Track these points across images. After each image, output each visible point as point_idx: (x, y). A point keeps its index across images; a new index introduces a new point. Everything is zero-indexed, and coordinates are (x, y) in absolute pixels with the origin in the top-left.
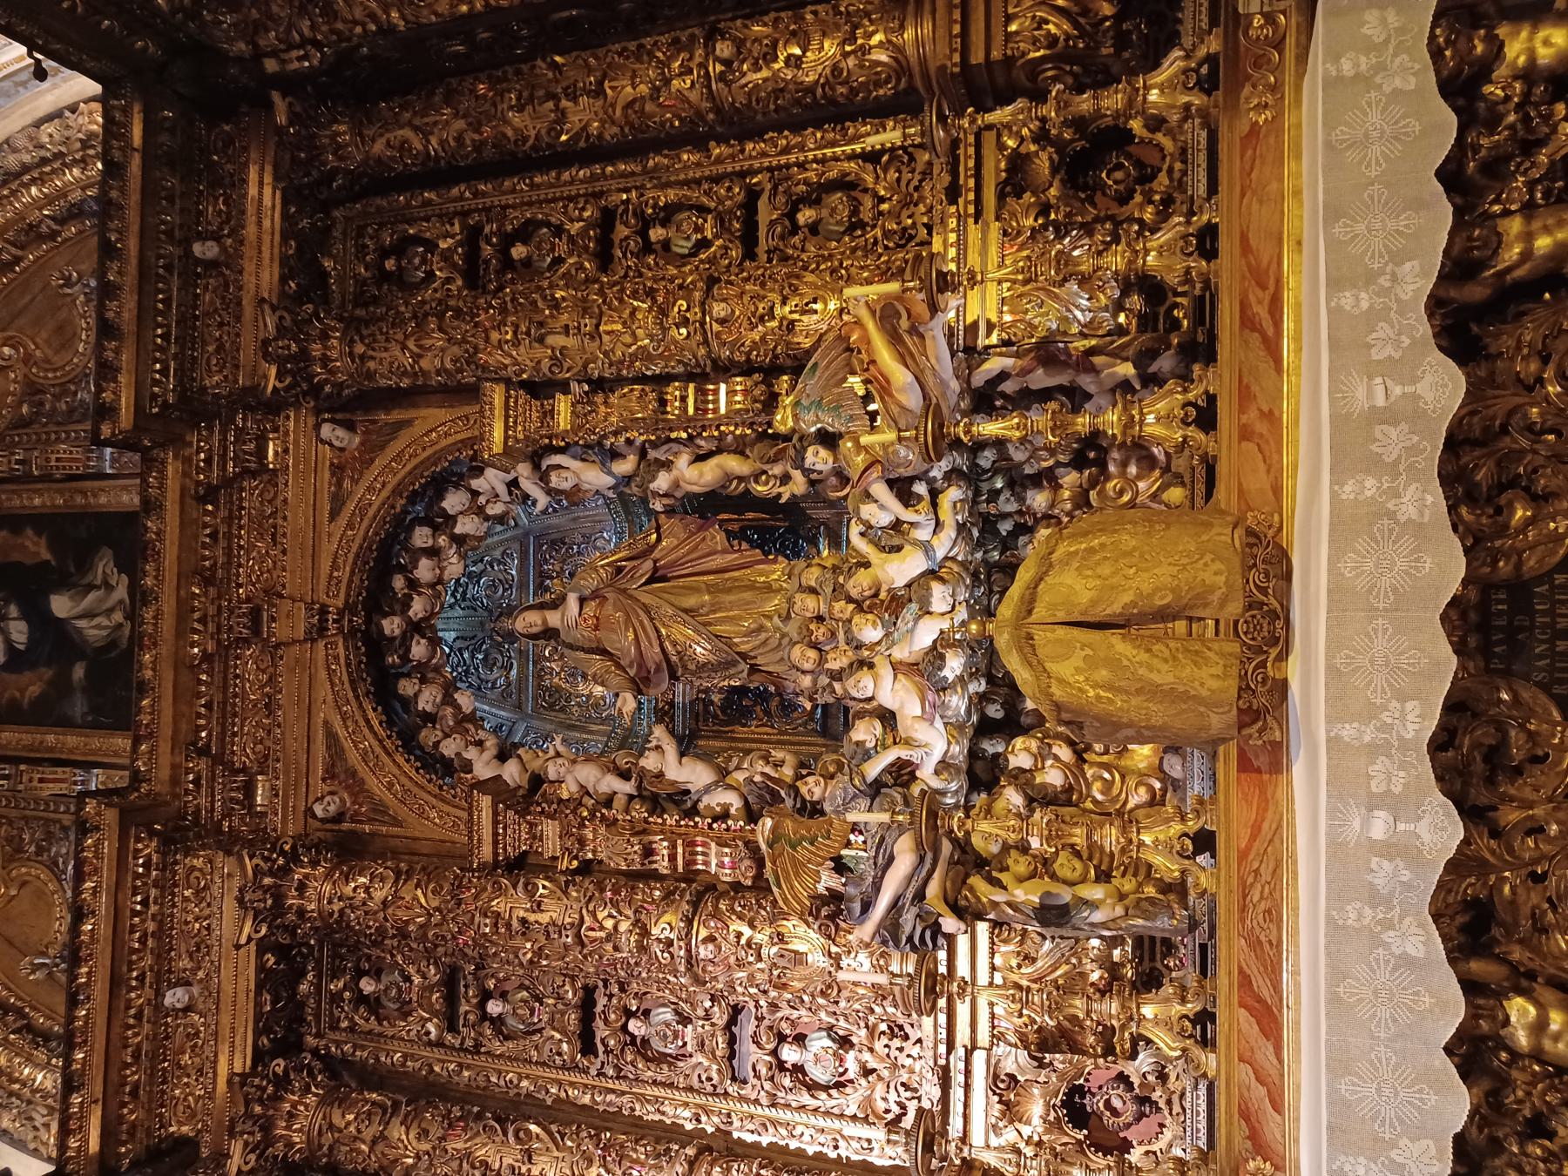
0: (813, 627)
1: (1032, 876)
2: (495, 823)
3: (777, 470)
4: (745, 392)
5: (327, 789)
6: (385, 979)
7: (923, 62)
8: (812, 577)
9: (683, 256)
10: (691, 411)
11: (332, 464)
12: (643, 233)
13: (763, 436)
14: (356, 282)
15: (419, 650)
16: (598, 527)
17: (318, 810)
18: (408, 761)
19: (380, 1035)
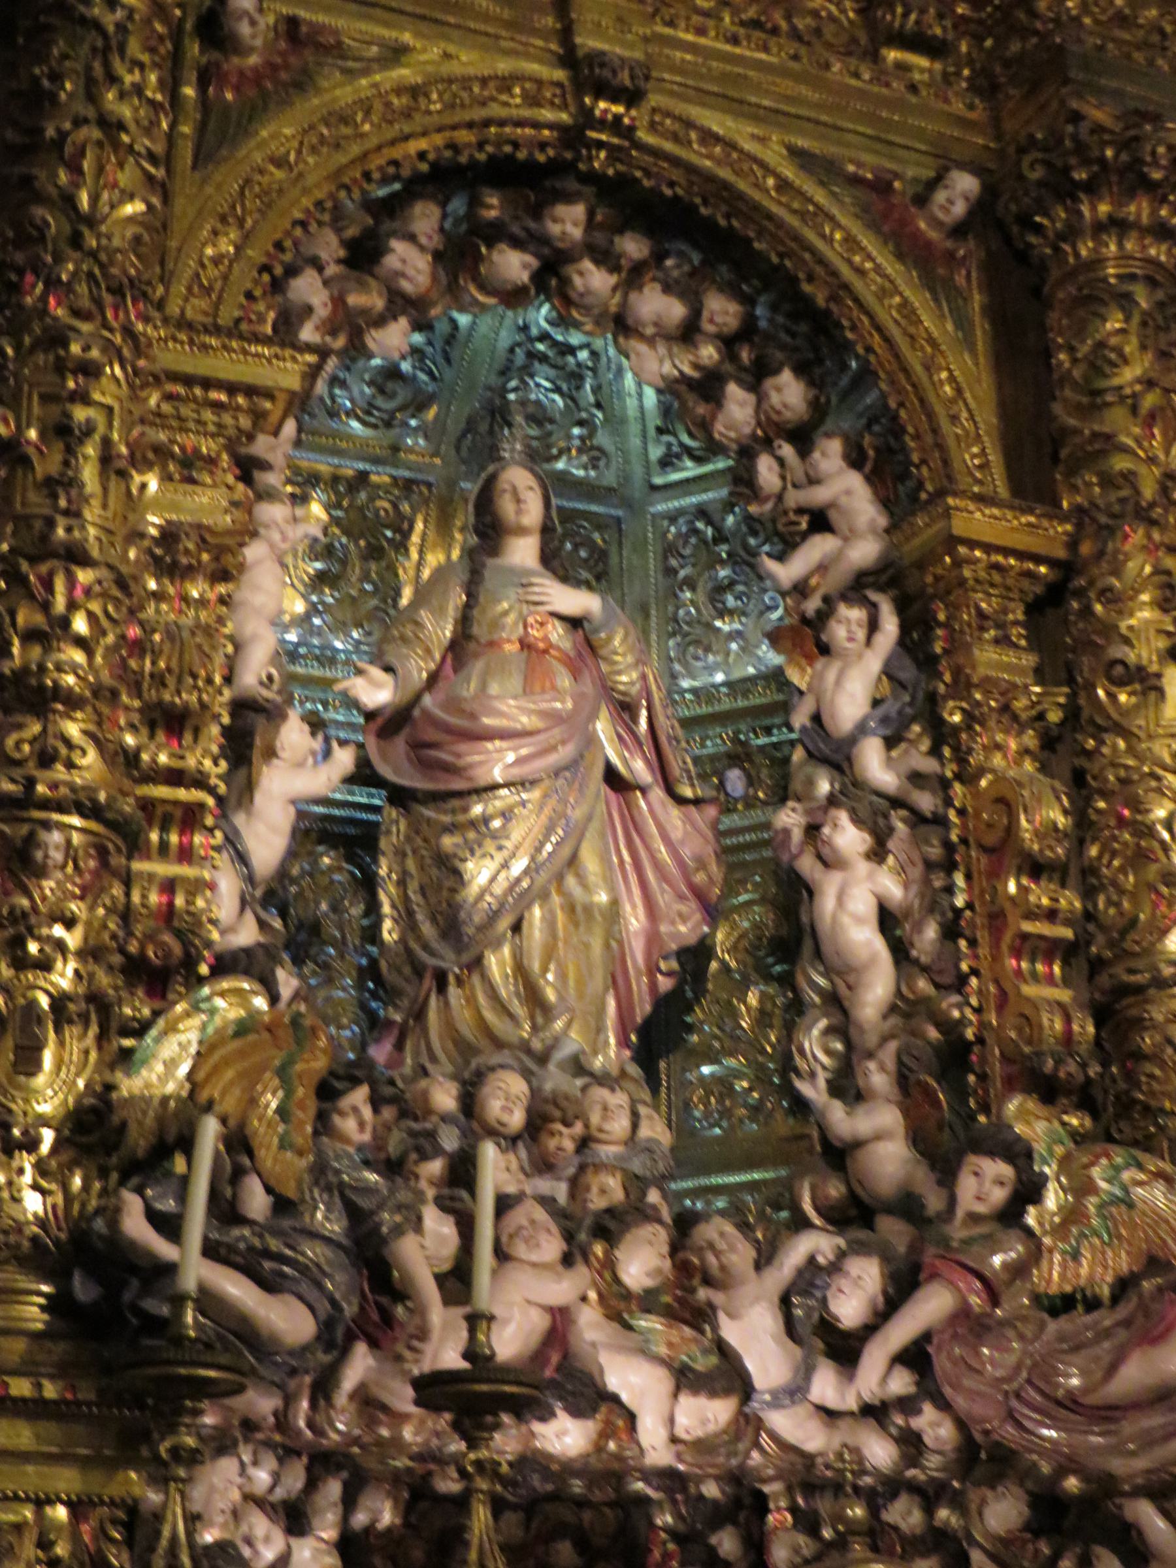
2: (232, 389)
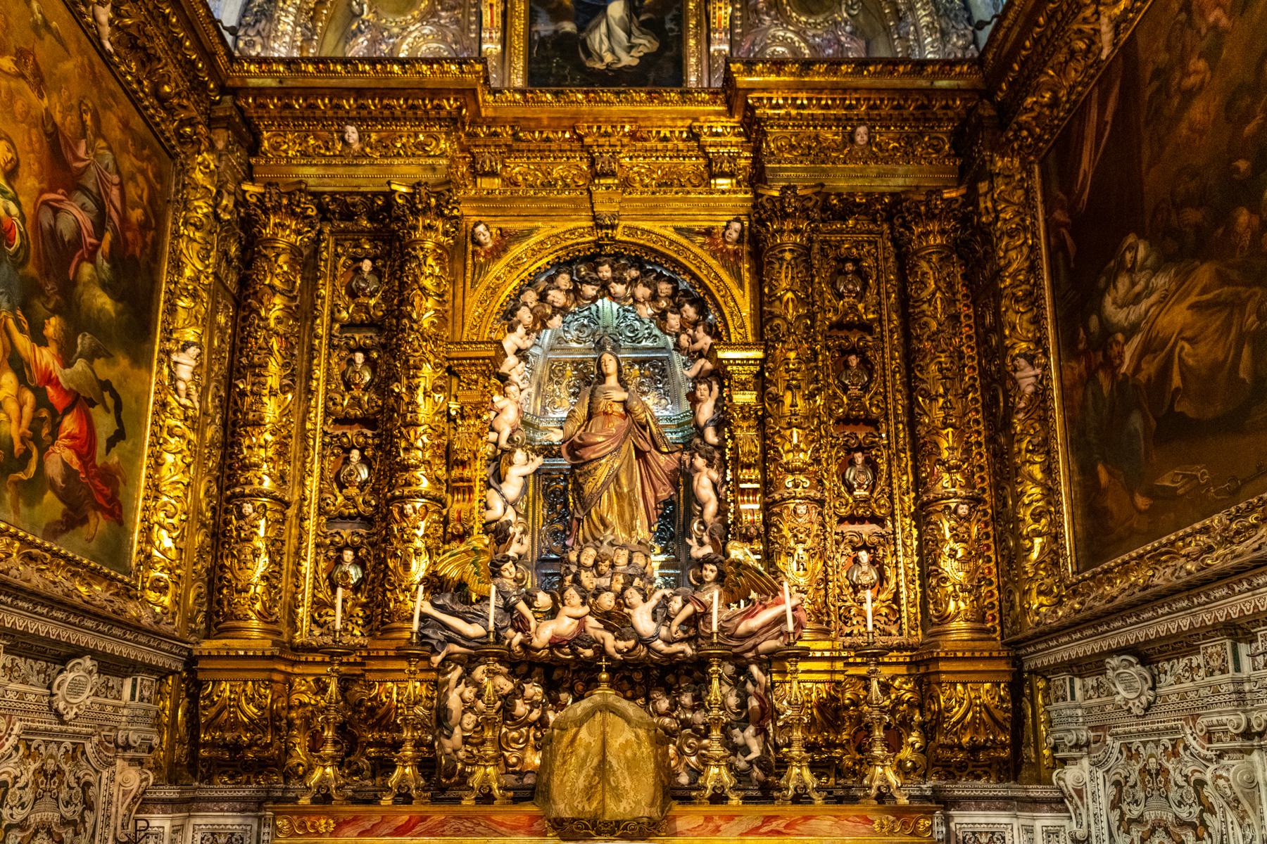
0: (607, 563)
1: (464, 701)
2: (478, 358)
3: (706, 539)
4: (753, 522)
5: (494, 231)
6: (371, 279)
7: (945, 633)
8: (639, 560)
9: (844, 475)
10: (742, 486)
12: (860, 449)
13: (727, 526)
17: (481, 228)
19: (335, 277)
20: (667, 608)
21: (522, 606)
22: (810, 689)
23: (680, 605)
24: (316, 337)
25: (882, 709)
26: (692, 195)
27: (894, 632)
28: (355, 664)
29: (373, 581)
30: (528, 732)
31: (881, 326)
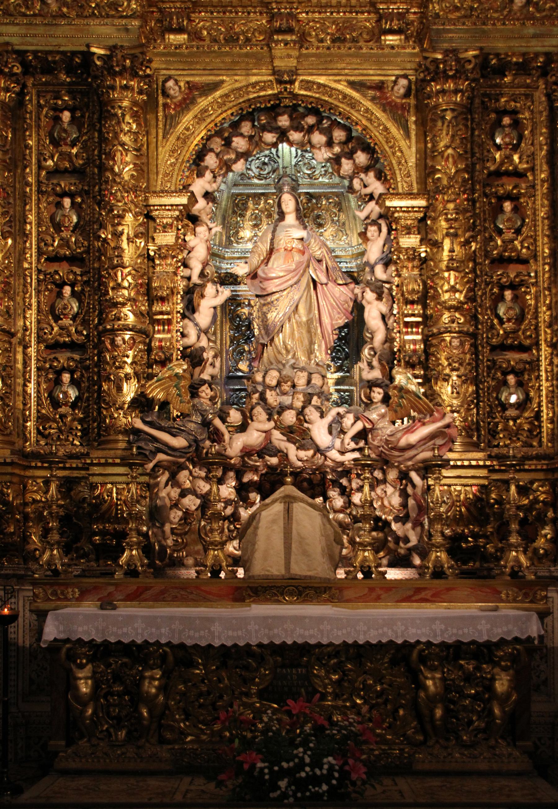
4: (415, 351)
5: (182, 84)
11: (383, 82)
14: (498, 95)
15: (270, 137)
16: (348, 232)
18: (202, 138)
20: (341, 423)
21: (217, 422)
22: (460, 491)
23: (352, 421)
24: (28, 184)
25: (519, 508)
26: (364, 51)
27: (535, 444)
28: (77, 468)
29: (88, 399)
30: (223, 525)
31: (534, 175)
